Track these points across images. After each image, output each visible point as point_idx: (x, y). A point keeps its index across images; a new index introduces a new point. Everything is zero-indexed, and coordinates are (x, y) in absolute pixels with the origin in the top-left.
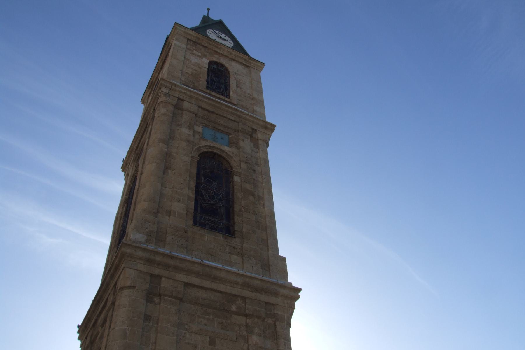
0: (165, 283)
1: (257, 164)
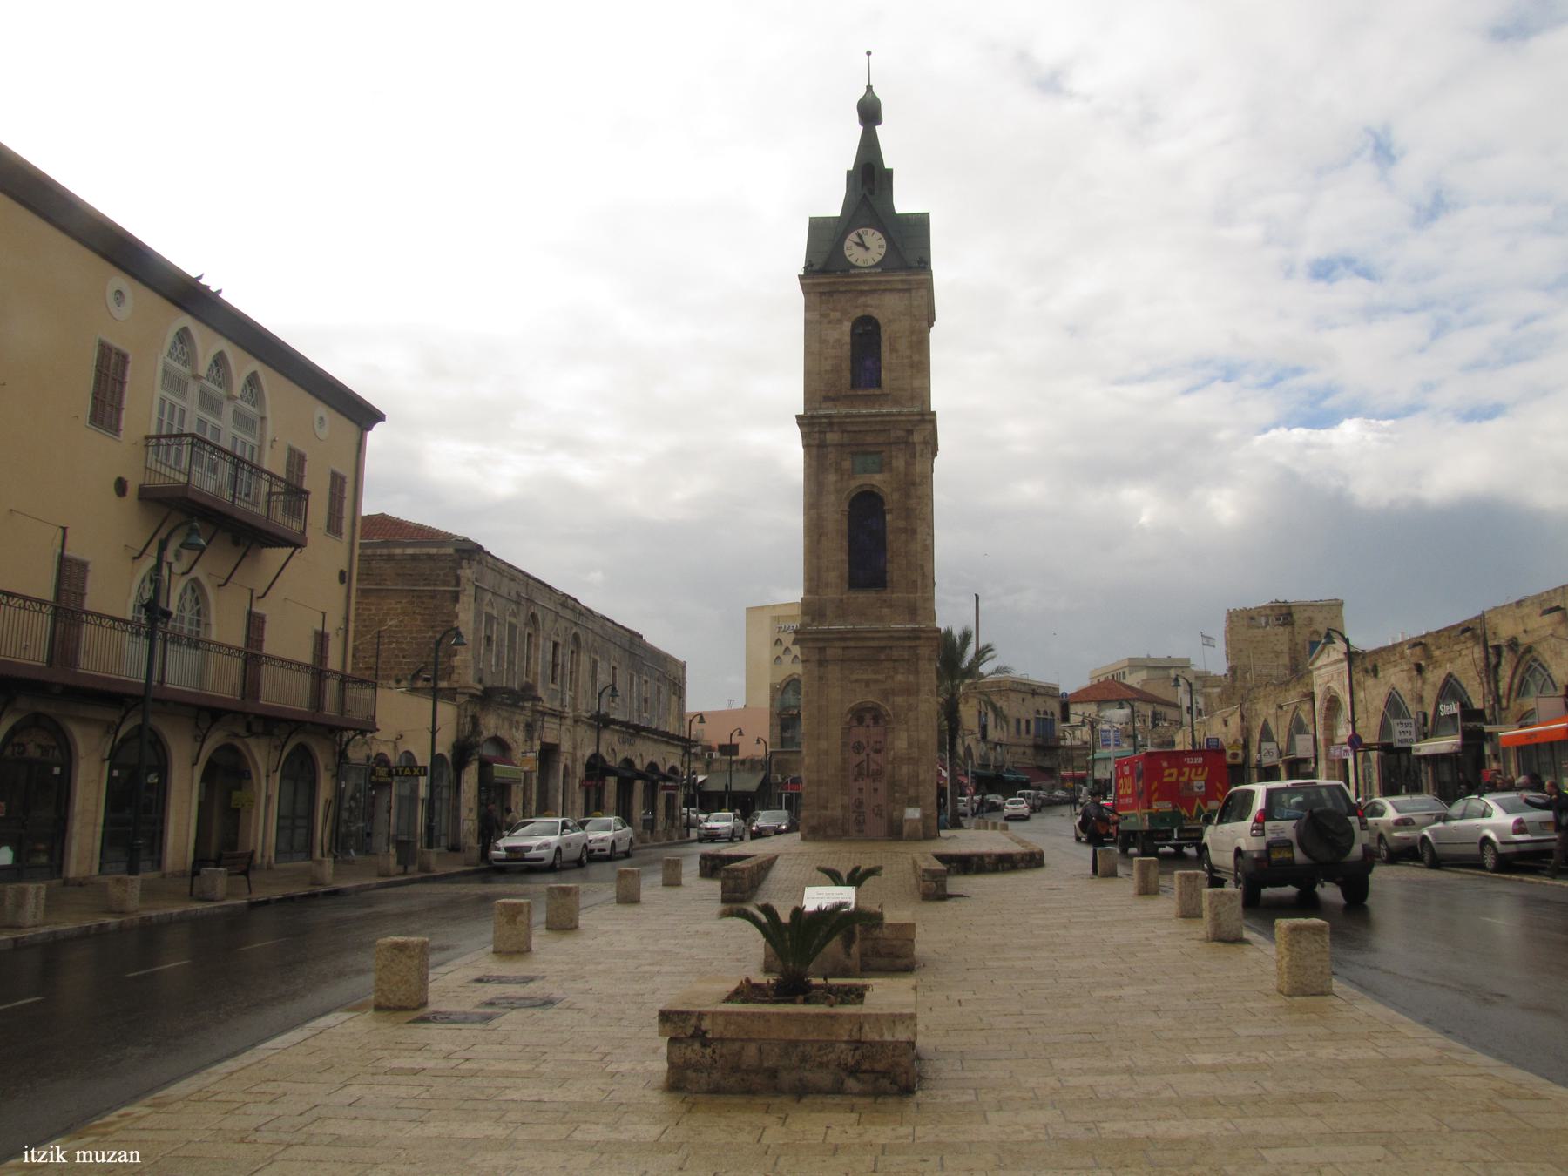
0: (829, 652)
1: (913, 484)
